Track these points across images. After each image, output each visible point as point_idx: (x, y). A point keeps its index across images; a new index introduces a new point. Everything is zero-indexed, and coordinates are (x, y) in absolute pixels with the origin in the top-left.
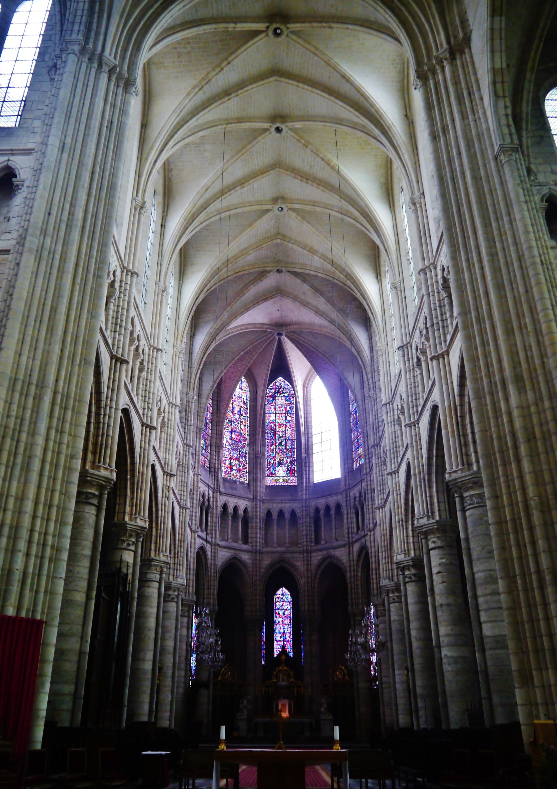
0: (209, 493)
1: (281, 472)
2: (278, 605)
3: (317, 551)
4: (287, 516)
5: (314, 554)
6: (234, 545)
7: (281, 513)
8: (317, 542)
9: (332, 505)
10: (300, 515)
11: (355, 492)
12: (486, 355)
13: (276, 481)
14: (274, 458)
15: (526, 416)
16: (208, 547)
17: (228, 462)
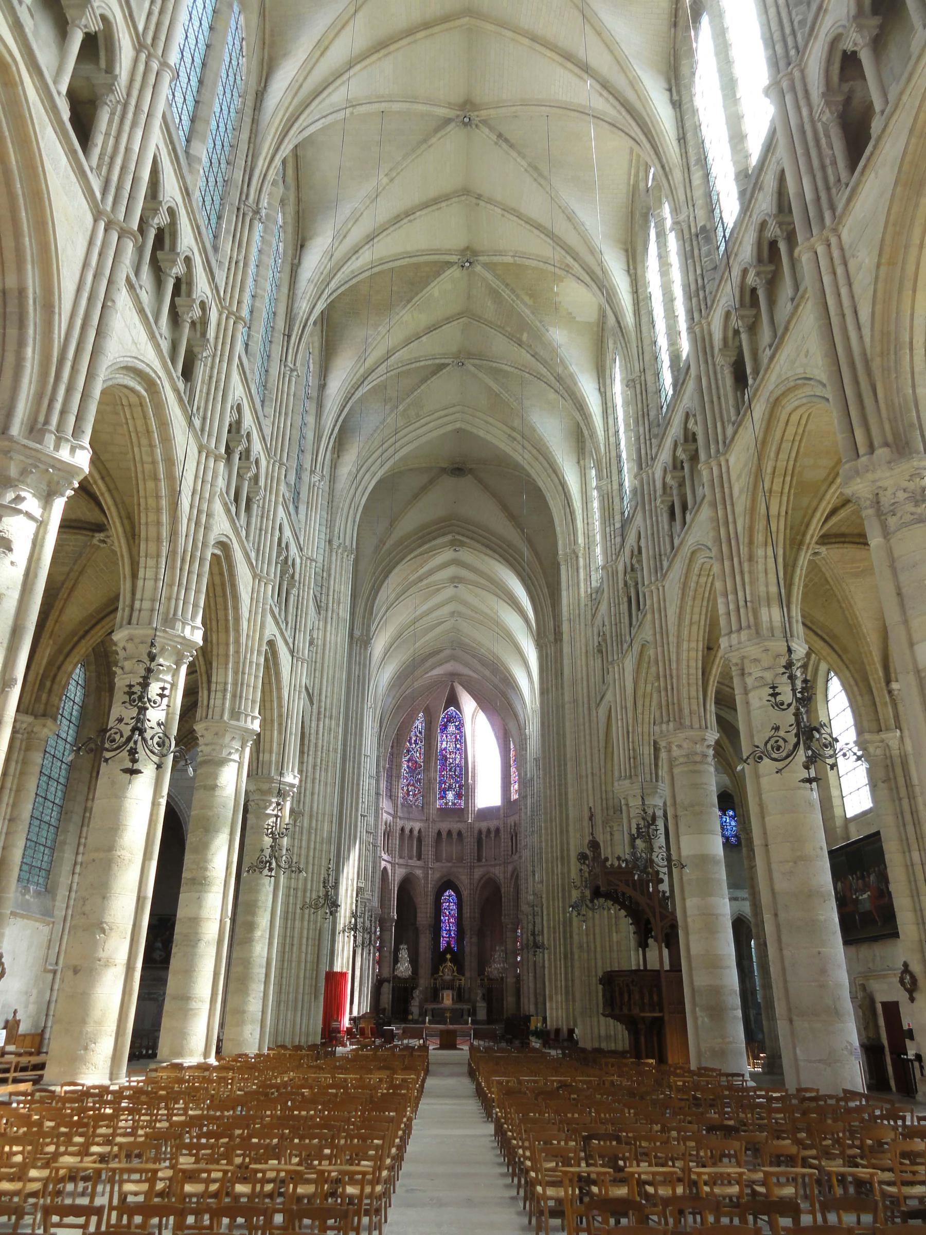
0: (390, 818)
1: (450, 795)
2: (445, 905)
3: (481, 866)
4: (455, 835)
5: (476, 870)
6: (412, 863)
7: (449, 833)
8: (479, 860)
9: (493, 829)
10: (465, 835)
11: (511, 821)
12: (552, 841)
13: (446, 804)
14: (445, 783)
15: (563, 879)
16: (389, 867)
17: (405, 789)
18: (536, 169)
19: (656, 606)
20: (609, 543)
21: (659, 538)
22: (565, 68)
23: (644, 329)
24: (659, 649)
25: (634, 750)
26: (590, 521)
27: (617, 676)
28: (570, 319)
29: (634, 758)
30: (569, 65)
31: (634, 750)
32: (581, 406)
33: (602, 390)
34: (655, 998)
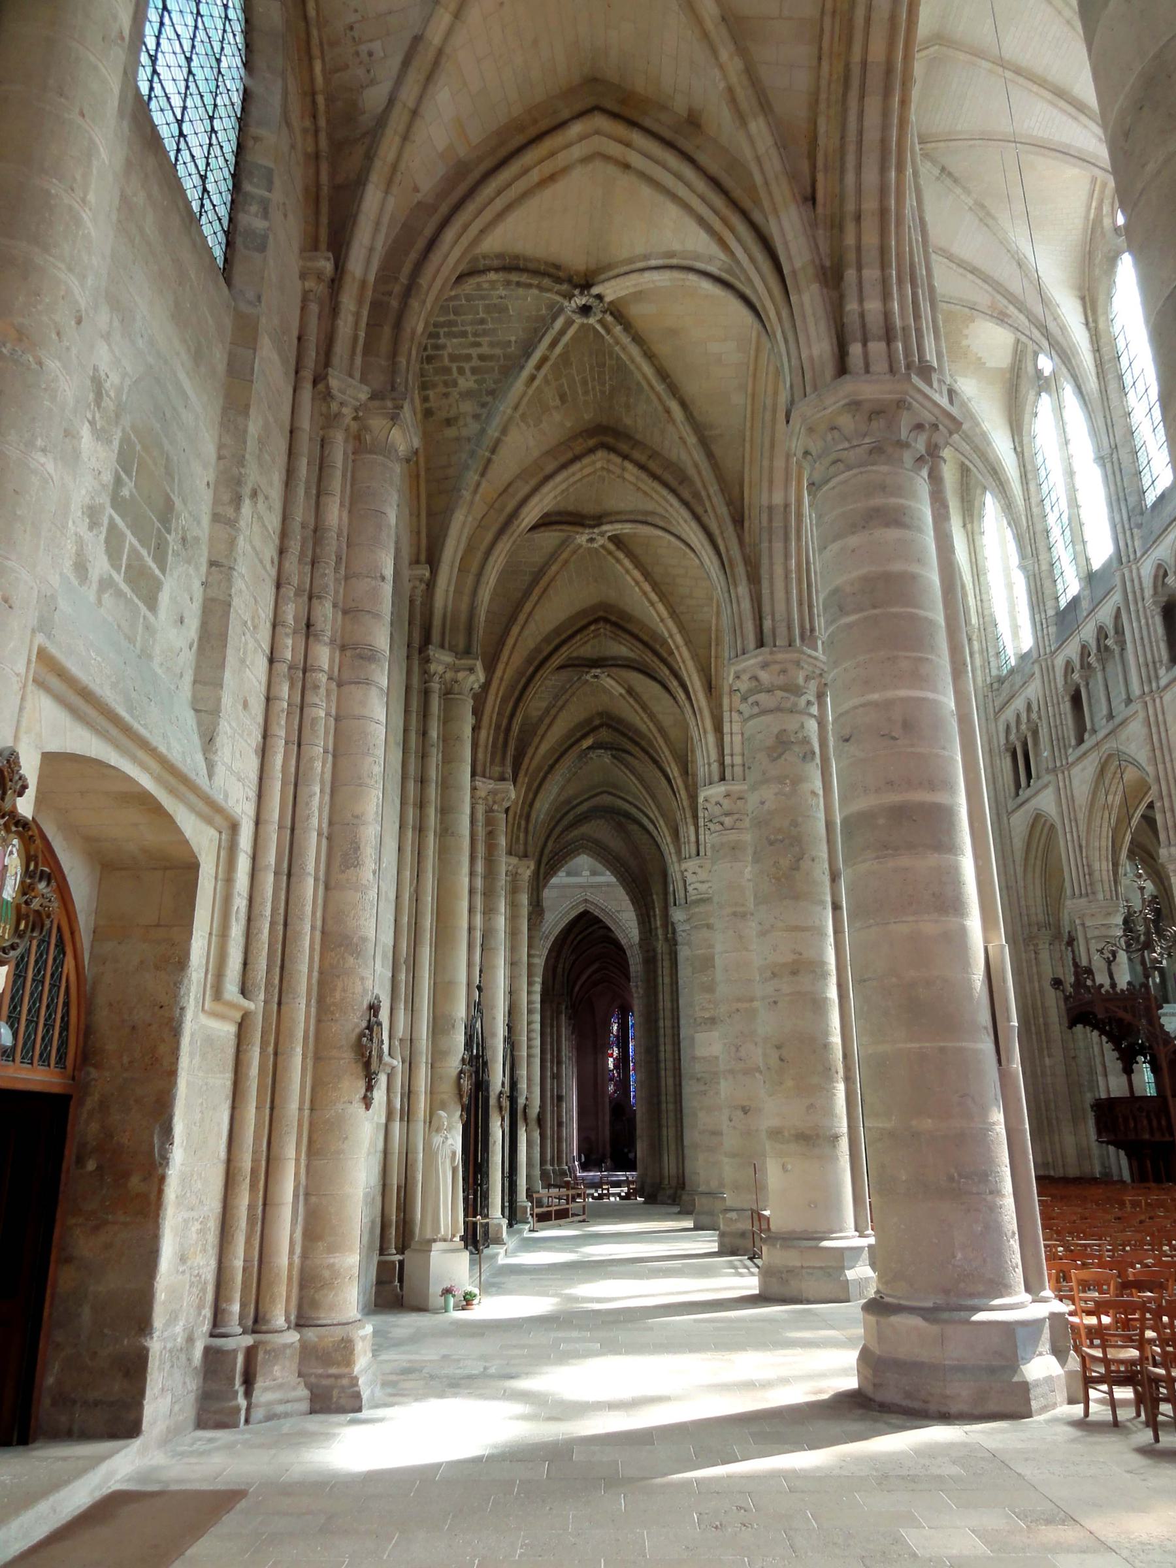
18: (982, 206)
19: (1152, 719)
20: (1039, 634)
21: (1151, 643)
22: (1056, 106)
23: (1113, 395)
24: (1160, 767)
25: (1089, 866)
26: (984, 597)
27: (1061, 784)
28: (979, 363)
29: (1090, 875)
30: (1062, 104)
31: (1089, 866)
32: (994, 469)
33: (1019, 449)
34: (1163, 1123)
